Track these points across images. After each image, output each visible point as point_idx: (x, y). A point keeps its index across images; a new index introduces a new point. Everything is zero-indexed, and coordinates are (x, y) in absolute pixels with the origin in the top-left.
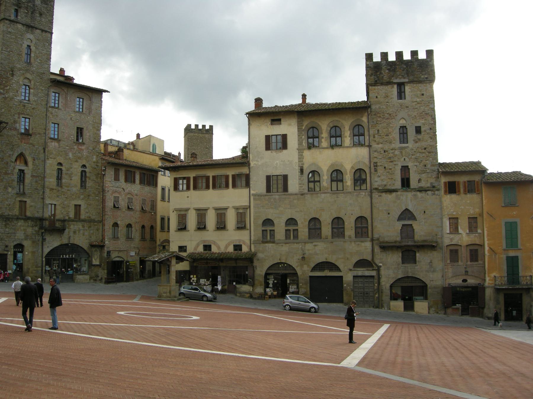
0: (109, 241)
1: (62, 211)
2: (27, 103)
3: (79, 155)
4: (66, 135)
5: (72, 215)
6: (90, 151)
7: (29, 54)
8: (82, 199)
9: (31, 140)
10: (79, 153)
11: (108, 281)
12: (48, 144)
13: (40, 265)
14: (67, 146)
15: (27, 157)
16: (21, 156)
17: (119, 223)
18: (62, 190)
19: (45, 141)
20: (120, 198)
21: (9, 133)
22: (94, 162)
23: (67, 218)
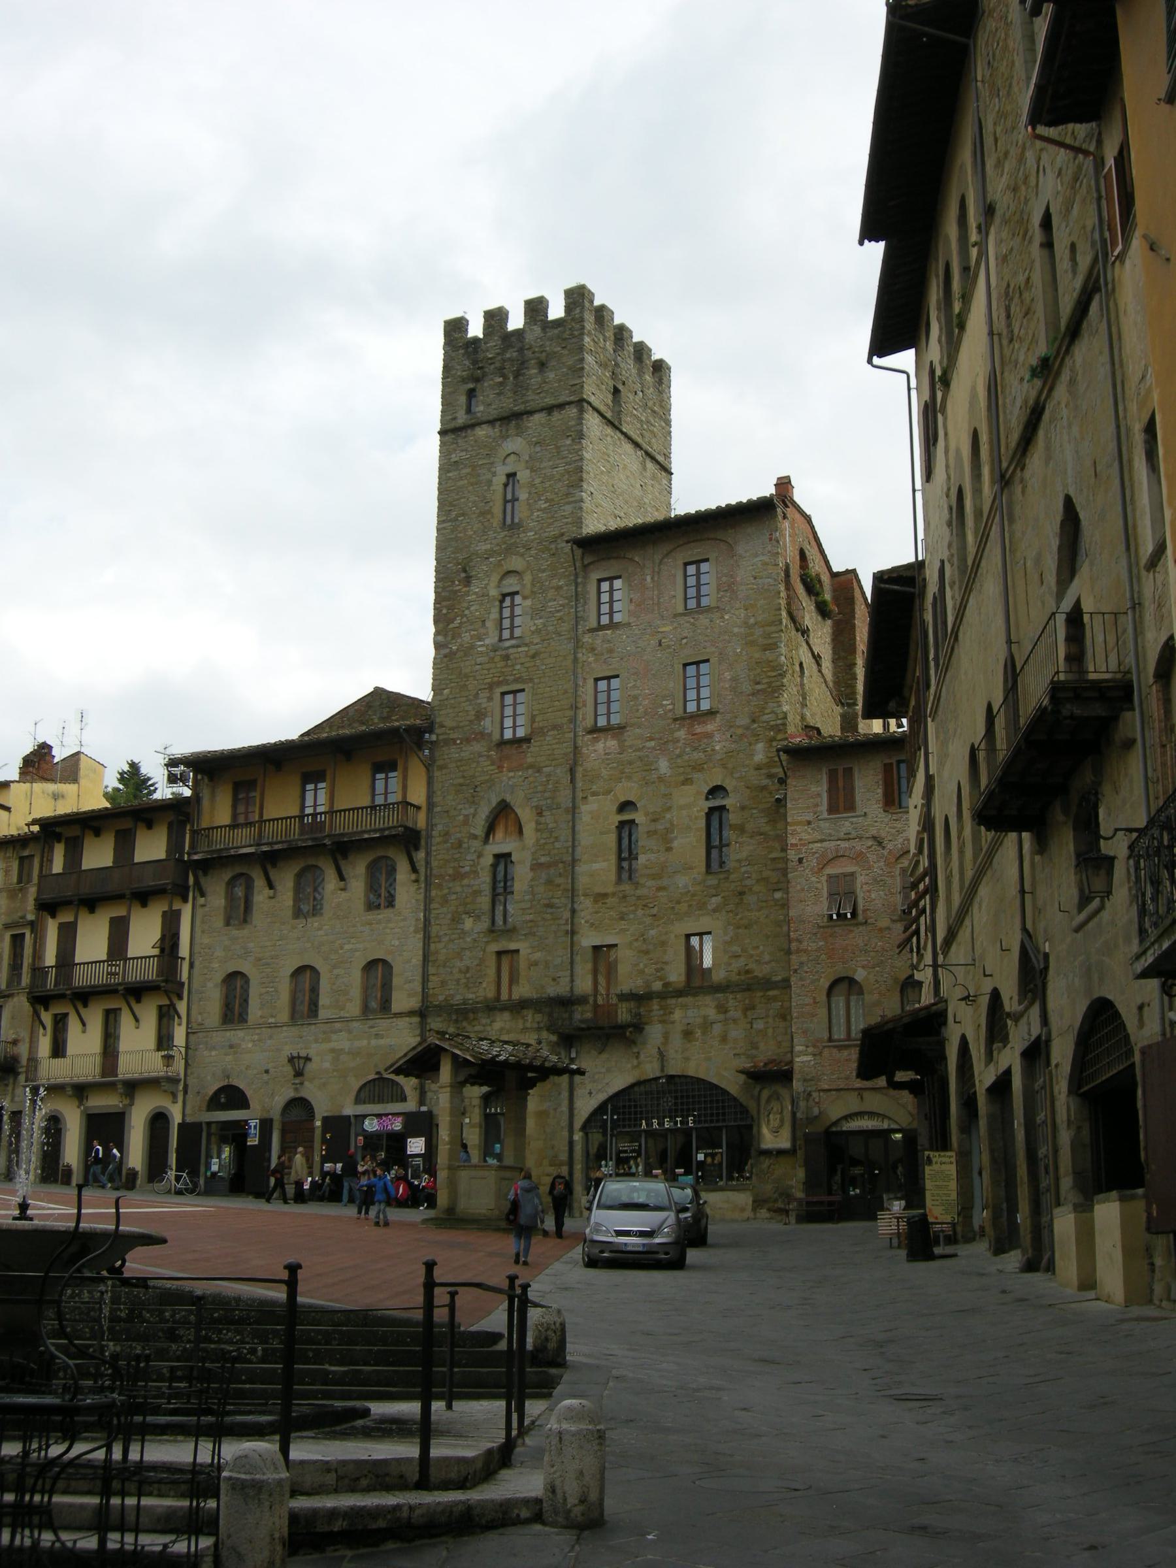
0: (814, 1055)
1: (641, 965)
2: (513, 647)
3: (698, 756)
4: (646, 702)
5: (676, 975)
6: (740, 731)
7: (510, 501)
8: (715, 911)
9: (529, 754)
10: (695, 749)
11: (812, 1214)
12: (585, 750)
13: (564, 1157)
14: (651, 739)
15: (519, 811)
16: (502, 812)
17: (860, 975)
18: (639, 892)
19: (575, 743)
20: (860, 879)
21: (463, 754)
22: (758, 768)
23: (657, 986)
